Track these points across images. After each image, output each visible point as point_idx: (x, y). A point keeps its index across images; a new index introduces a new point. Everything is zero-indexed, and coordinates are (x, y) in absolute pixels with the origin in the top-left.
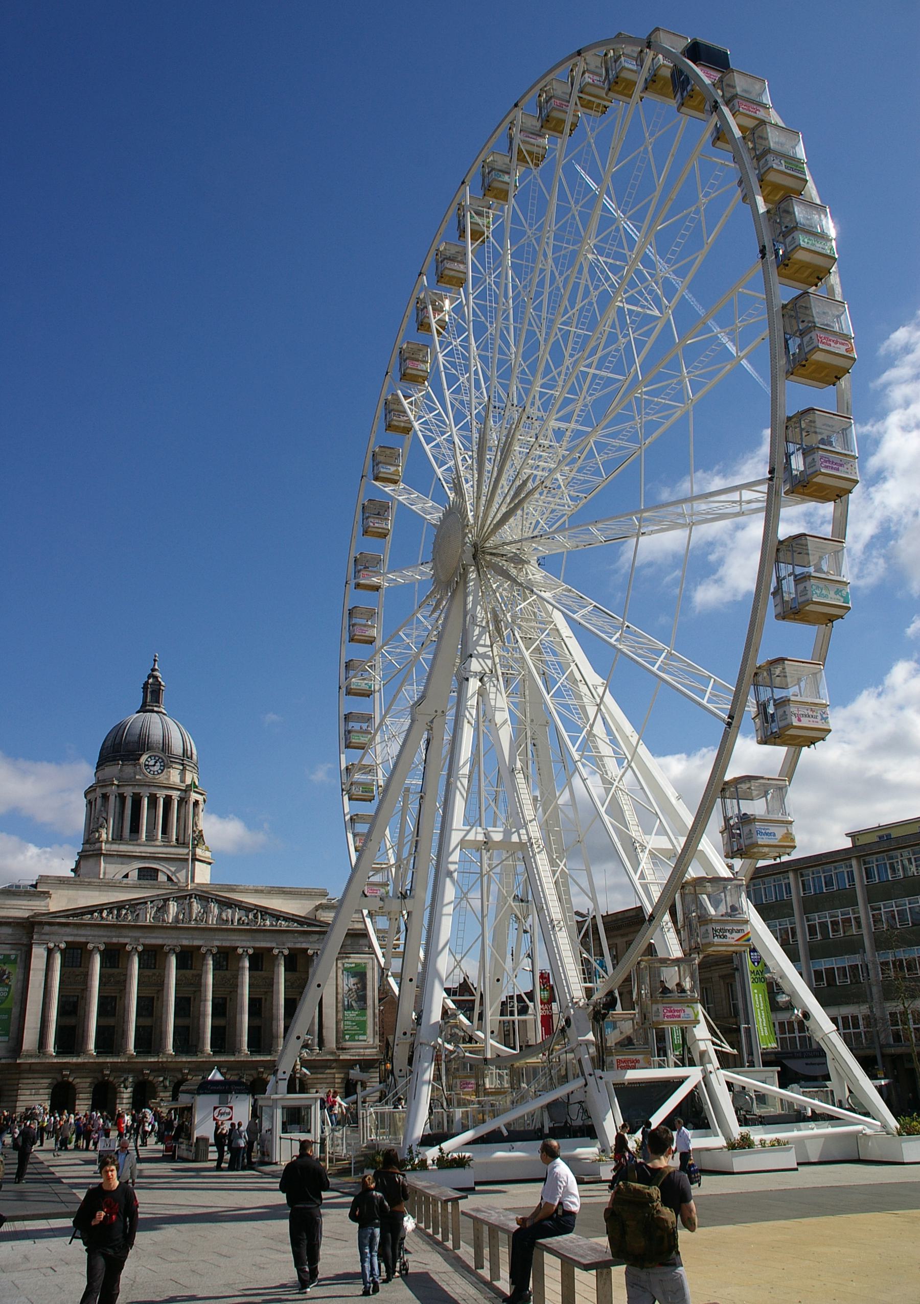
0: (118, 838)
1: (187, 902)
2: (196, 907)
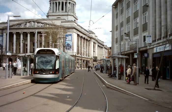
0: (53, 12)
1: (31, 23)
2: (33, 23)
